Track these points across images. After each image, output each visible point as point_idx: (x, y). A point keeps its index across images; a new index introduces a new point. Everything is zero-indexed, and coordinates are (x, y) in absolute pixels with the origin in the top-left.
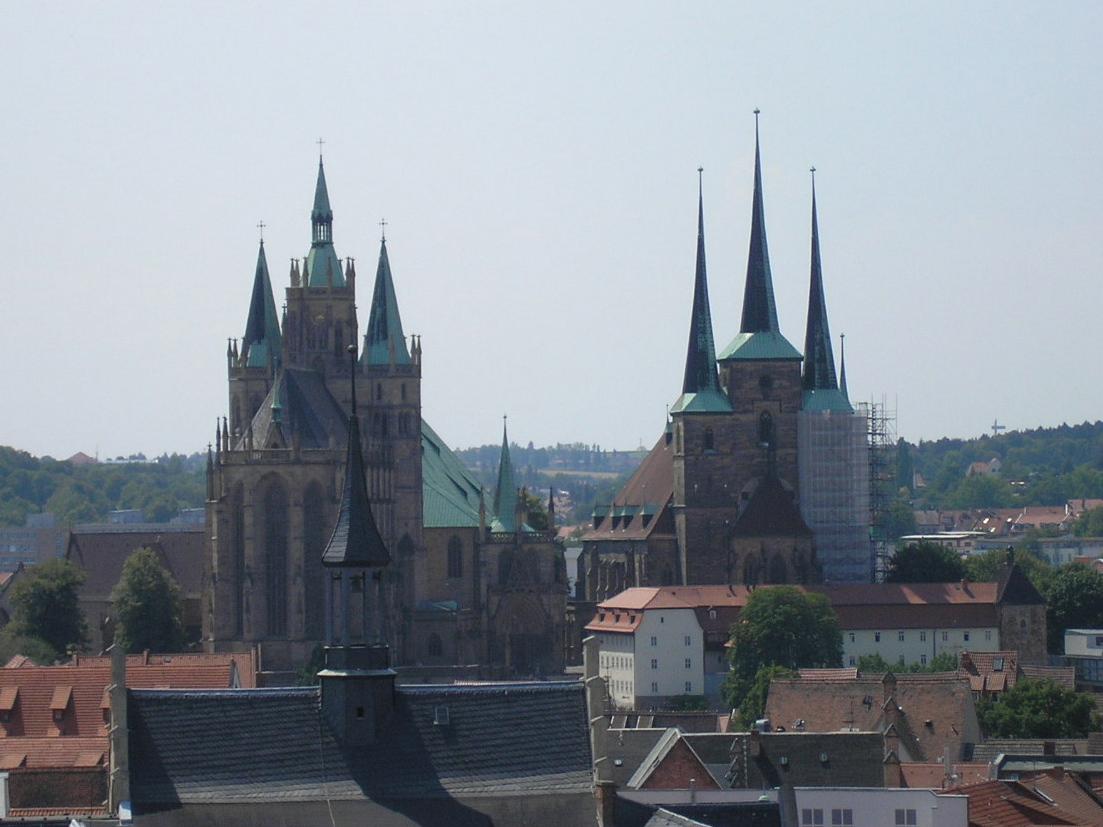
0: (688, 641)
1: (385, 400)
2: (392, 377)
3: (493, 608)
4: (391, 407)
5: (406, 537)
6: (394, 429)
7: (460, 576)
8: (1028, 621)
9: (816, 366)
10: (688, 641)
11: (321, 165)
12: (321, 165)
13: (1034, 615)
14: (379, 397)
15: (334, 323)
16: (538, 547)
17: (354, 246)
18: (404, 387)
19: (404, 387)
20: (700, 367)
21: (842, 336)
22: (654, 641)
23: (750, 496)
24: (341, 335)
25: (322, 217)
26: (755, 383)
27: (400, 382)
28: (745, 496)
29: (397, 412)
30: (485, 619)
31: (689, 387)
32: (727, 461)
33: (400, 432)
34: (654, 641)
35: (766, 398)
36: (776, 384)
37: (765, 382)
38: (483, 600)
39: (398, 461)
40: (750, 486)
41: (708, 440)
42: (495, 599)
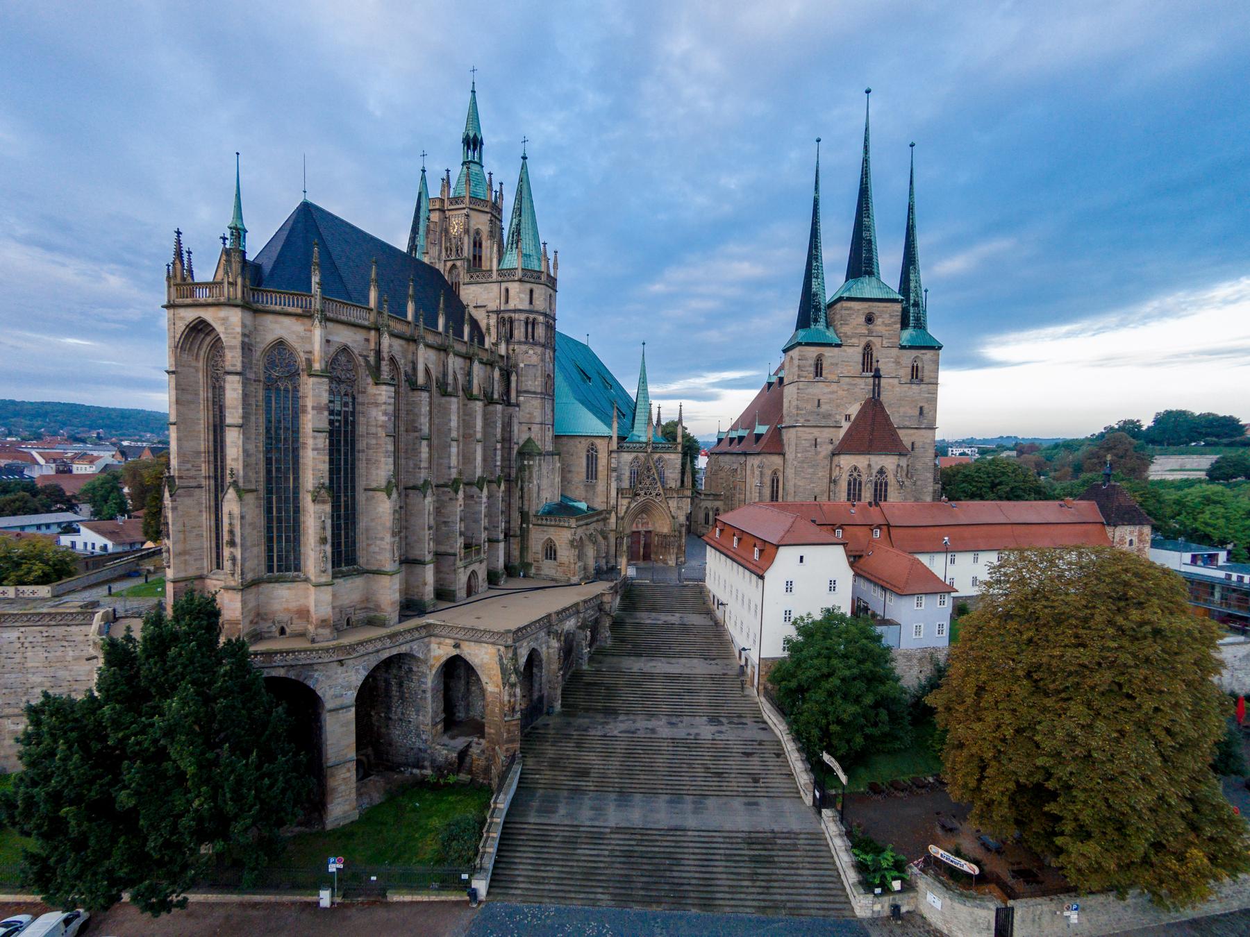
0: (832, 586)
1: (511, 306)
4: (515, 311)
5: (529, 439)
6: (519, 333)
8: (1135, 540)
9: (912, 310)
10: (832, 586)
13: (1141, 534)
14: (507, 302)
16: (666, 456)
17: (500, 170)
18: (531, 291)
19: (531, 291)
22: (789, 586)
23: (853, 418)
24: (480, 246)
25: (473, 143)
26: (862, 319)
27: (529, 286)
28: (848, 417)
29: (523, 317)
30: (613, 519)
32: (834, 387)
33: (527, 337)
34: (789, 586)
35: (870, 333)
36: (879, 321)
37: (869, 319)
38: (613, 502)
39: (522, 365)
40: (854, 410)
41: (818, 370)
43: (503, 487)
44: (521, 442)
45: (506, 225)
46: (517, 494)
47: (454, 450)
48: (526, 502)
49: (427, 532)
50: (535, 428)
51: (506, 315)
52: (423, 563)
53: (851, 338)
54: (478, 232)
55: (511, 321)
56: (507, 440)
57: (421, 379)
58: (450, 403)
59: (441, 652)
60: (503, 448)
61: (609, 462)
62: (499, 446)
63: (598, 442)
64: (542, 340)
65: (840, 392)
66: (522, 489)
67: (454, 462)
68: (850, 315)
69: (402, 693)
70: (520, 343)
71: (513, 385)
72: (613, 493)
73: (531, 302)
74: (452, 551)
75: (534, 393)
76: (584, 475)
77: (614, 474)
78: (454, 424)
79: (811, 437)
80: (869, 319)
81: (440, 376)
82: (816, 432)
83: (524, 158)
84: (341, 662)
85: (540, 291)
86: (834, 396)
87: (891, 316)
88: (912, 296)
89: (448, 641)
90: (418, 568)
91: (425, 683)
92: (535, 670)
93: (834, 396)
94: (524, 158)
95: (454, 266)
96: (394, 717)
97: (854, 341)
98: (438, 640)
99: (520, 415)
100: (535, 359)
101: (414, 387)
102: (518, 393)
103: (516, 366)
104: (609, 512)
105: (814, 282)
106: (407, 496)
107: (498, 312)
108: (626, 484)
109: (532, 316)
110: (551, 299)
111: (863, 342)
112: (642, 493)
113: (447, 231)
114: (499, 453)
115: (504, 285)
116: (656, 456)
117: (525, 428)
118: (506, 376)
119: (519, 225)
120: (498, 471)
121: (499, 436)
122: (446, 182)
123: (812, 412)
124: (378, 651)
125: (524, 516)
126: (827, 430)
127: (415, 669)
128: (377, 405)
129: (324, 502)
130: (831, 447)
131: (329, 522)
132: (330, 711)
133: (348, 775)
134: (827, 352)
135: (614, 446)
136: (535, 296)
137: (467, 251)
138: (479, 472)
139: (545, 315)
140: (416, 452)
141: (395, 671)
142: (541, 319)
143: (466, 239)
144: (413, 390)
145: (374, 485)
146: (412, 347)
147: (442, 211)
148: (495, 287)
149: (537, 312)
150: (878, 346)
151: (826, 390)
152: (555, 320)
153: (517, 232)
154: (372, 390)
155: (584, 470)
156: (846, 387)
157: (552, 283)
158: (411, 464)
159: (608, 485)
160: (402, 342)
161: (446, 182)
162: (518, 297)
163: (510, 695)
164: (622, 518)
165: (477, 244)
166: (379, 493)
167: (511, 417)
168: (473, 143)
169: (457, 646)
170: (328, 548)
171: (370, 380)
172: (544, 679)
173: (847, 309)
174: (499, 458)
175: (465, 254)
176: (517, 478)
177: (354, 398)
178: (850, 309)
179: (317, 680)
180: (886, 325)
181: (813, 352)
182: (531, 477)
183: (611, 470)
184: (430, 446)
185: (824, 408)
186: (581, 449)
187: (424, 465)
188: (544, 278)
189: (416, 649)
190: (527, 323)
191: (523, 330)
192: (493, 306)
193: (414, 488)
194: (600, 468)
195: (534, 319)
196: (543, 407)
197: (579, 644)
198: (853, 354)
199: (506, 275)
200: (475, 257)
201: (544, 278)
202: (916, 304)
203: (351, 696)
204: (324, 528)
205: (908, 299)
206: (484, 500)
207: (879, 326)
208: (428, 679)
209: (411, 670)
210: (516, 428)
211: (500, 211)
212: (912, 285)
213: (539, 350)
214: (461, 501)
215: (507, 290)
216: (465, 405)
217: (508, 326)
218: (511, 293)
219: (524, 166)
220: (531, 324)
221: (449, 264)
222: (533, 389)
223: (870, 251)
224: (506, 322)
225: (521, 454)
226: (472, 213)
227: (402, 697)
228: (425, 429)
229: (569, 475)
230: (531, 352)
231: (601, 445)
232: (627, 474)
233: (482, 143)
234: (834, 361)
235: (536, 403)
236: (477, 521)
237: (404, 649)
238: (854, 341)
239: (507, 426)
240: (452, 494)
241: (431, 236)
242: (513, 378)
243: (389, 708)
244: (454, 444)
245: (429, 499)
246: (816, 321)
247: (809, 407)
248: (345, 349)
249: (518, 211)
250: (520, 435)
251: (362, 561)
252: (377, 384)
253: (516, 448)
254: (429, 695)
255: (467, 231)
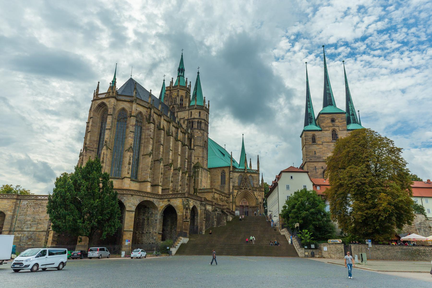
1: (193, 117)
2: (196, 109)
3: (235, 194)
4: (194, 118)
6: (195, 126)
7: (225, 184)
9: (351, 117)
11: (182, 56)
12: (182, 56)
14: (191, 116)
15: (180, 97)
16: (253, 175)
17: (190, 77)
18: (200, 113)
19: (200, 113)
20: (309, 118)
21: (359, 111)
26: (329, 121)
27: (199, 111)
29: (196, 120)
30: (231, 198)
31: (306, 124)
32: (321, 146)
33: (198, 127)
34: (288, 187)
35: (334, 125)
36: (337, 121)
37: (333, 120)
38: (231, 191)
39: (196, 136)
41: (314, 140)
42: (236, 191)
43: (187, 175)
44: (195, 163)
45: (192, 94)
46: (193, 181)
47: (171, 153)
48: (196, 185)
49: (160, 175)
50: (200, 159)
51: (191, 120)
52: (159, 185)
53: (326, 127)
54: (182, 96)
55: (193, 122)
56: (190, 162)
57: (162, 127)
58: (170, 138)
59: (163, 204)
60: (188, 162)
61: (229, 176)
62: (186, 160)
63: (225, 169)
64: (203, 128)
65: (324, 148)
66: (195, 180)
67: (170, 157)
68: (324, 119)
69: (148, 222)
70: (195, 129)
71: (192, 142)
72: (231, 187)
73: (200, 116)
74: (167, 188)
75: (200, 146)
76: (220, 183)
77: (231, 180)
78: (171, 145)
79: (313, 166)
80: (333, 120)
81: (168, 131)
82: (315, 164)
83: (198, 73)
84: (132, 195)
85: (202, 112)
86: (321, 150)
87: (342, 119)
88: (351, 112)
89: (166, 200)
90: (156, 188)
91: (157, 217)
92: (195, 217)
93: (321, 150)
94: (198, 73)
95: (173, 107)
96: (144, 232)
97: (327, 129)
98: (162, 200)
99: (194, 153)
100: (200, 135)
101: (159, 129)
102: (194, 146)
103: (194, 136)
104: (229, 195)
105: (309, 109)
106: (154, 163)
107: (188, 120)
108: (236, 185)
109: (200, 120)
110: (207, 116)
111: (331, 129)
112: (243, 188)
113: (171, 96)
114: (186, 163)
115: (190, 111)
116: (249, 175)
117: (196, 158)
118: (190, 139)
119: (196, 93)
120: (186, 170)
121: (187, 157)
122: (172, 82)
123: (312, 157)
124: (144, 196)
125: (194, 189)
126: (320, 163)
127: (154, 212)
128: (148, 129)
129: (131, 152)
130: (322, 170)
131: (132, 159)
132: (127, 211)
133: (130, 236)
134: (316, 133)
135: (231, 169)
136: (201, 114)
137: (178, 102)
138: (179, 166)
139: (204, 120)
140: (158, 149)
141: (146, 215)
142: (203, 121)
143: (178, 98)
144: (159, 130)
145: (145, 153)
146: (160, 117)
147: (170, 90)
148: (187, 112)
149: (202, 119)
150: (338, 130)
151: (318, 148)
152: (208, 123)
153: (195, 95)
154: (147, 125)
155: (220, 181)
156: (326, 146)
157: (207, 111)
158: (157, 153)
159: (229, 185)
160: (157, 116)
161: (172, 82)
162: (195, 114)
163: (186, 212)
164: (235, 198)
165: (182, 100)
166: (147, 156)
167: (191, 153)
168: (181, 70)
169: (169, 201)
170: (131, 166)
171: (147, 122)
172: (199, 221)
173: (322, 117)
174: (186, 165)
175: (177, 103)
176: (193, 175)
177: (141, 128)
178: (324, 117)
179: (125, 200)
180: (340, 122)
181: (311, 134)
182: (198, 175)
183: (230, 178)
184: (163, 148)
185: (318, 154)
186: (219, 173)
187: (161, 153)
188: (204, 108)
189: (155, 201)
190: (198, 123)
191: (196, 124)
192: (186, 118)
193: (157, 160)
194: (226, 179)
195: (201, 121)
196: (203, 151)
197: (213, 217)
198: (328, 134)
199: (191, 108)
200: (180, 104)
201: (204, 108)
202: (353, 115)
203: (134, 208)
204: (130, 159)
205: (349, 113)
206: (180, 175)
207: (337, 123)
208: (158, 216)
209: (152, 213)
210: (193, 158)
211: (190, 90)
212: (350, 108)
213: (202, 132)
214: (172, 170)
215: (191, 112)
216: (175, 143)
217: (191, 124)
218: (193, 113)
219: (198, 76)
220: (200, 123)
221: (171, 106)
222: (200, 145)
223: (330, 97)
224: (191, 122)
225: (195, 167)
226: (180, 90)
227: (148, 224)
228: (162, 142)
229: (214, 184)
230: (199, 132)
231: (227, 170)
232: (237, 181)
233: (184, 70)
234: (319, 136)
235: (201, 149)
236: (178, 183)
237: (151, 200)
238: (327, 129)
239: (190, 156)
240: (169, 168)
241: (166, 99)
242: (193, 140)
243: (143, 229)
244: (171, 151)
245: (161, 164)
246: (311, 123)
247: (311, 154)
248: (140, 113)
249: (196, 89)
250: (194, 160)
251: (139, 178)
252: (149, 123)
253: (193, 165)
254: (158, 221)
255: (178, 96)
